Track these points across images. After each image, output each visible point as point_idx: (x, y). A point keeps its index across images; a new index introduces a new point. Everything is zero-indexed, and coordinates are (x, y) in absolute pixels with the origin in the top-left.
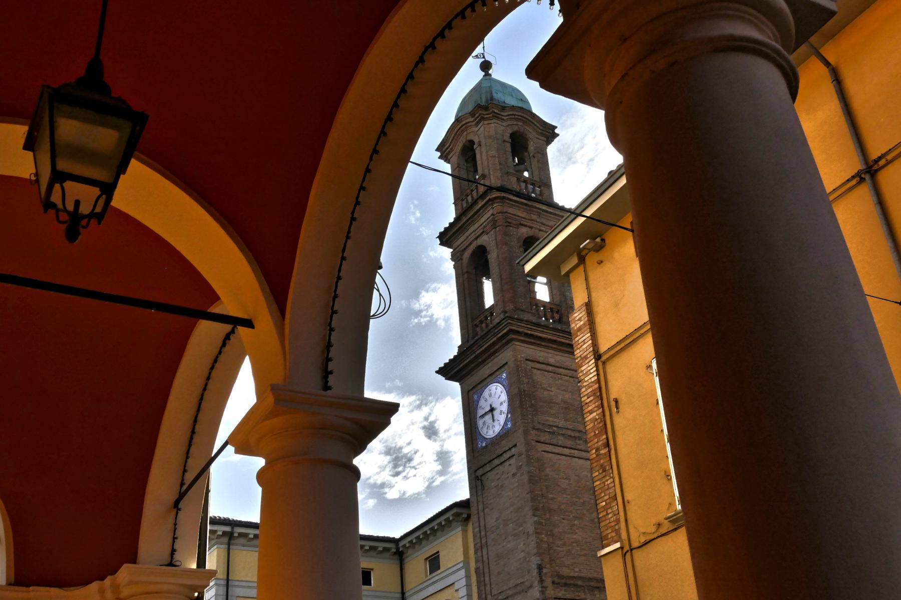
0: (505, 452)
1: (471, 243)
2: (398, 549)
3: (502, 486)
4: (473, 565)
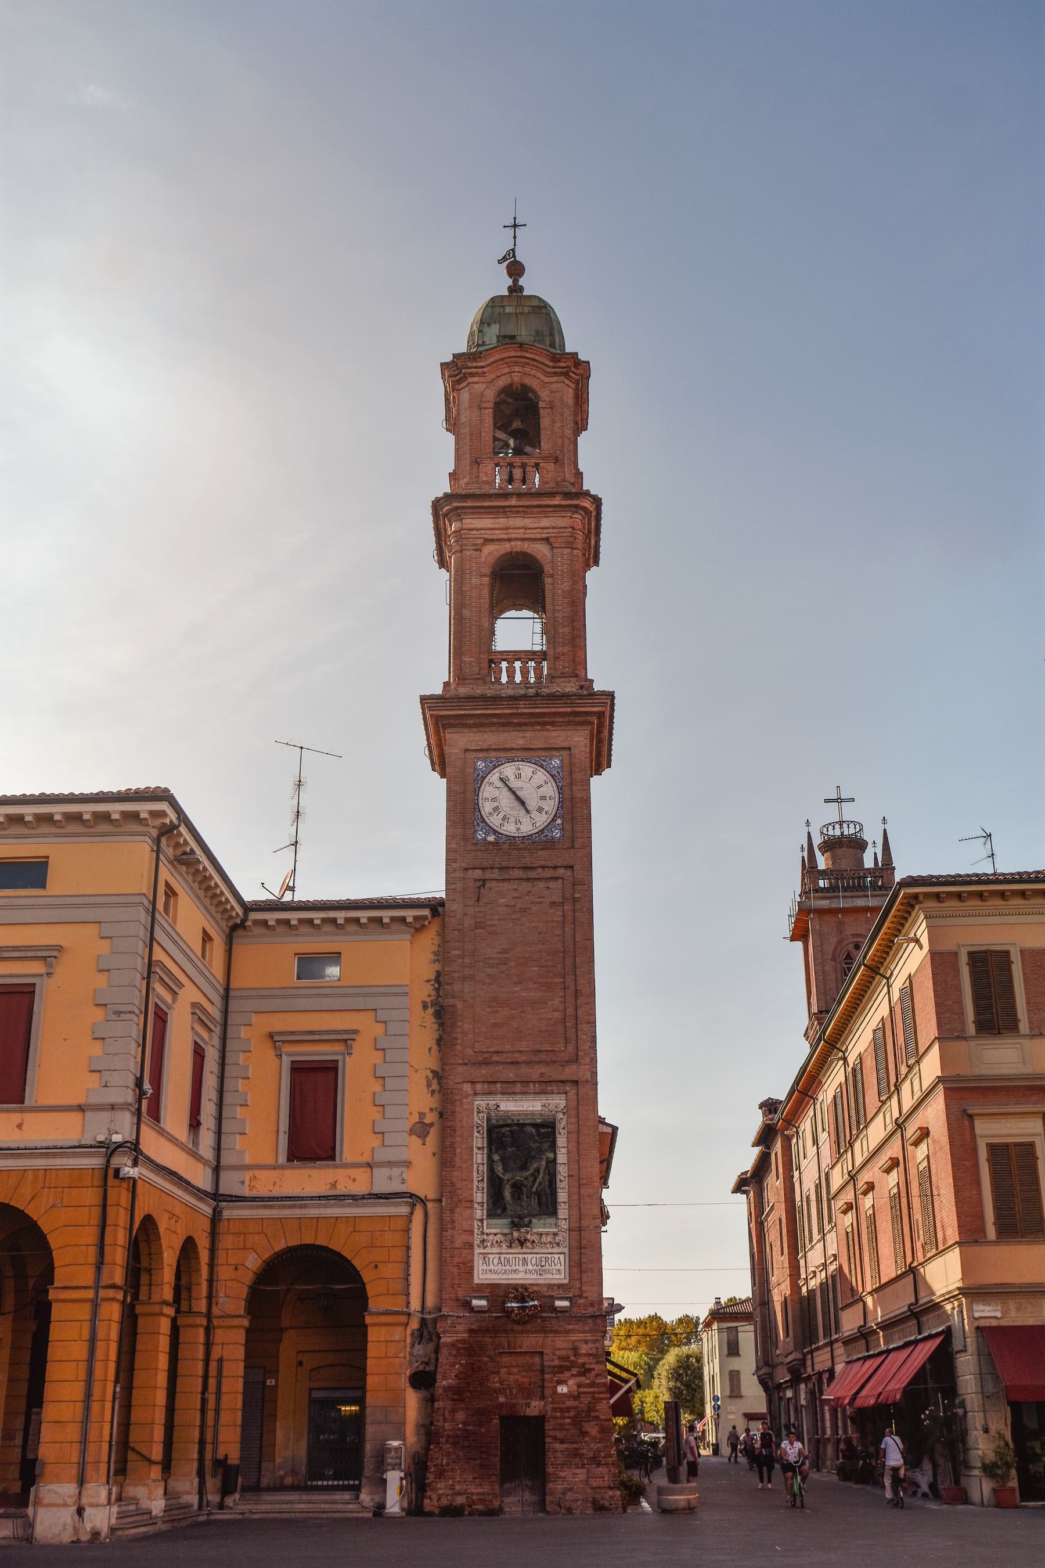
0: (543, 867)
1: (509, 540)
3: (523, 910)
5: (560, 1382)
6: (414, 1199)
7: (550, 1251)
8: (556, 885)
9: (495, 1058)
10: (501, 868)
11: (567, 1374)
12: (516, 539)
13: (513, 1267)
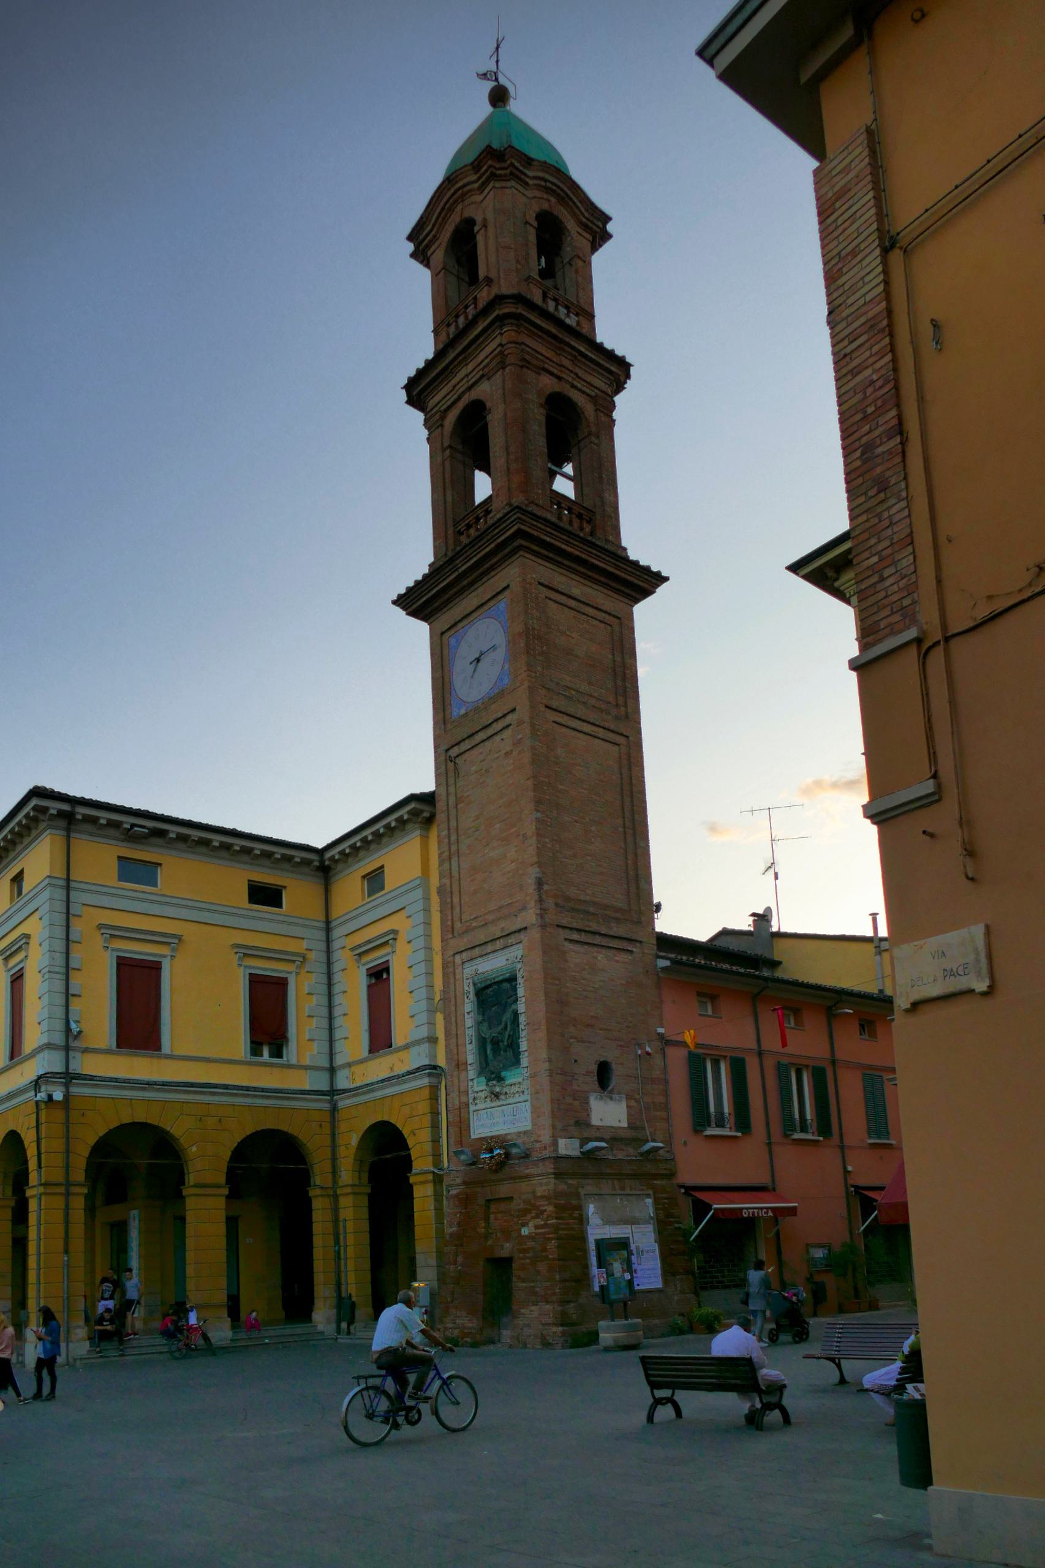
0: (496, 720)
1: (459, 398)
3: (487, 771)
4: (435, 881)
5: (524, 1225)
8: (507, 734)
10: (469, 737)
11: (528, 1217)
12: (463, 393)
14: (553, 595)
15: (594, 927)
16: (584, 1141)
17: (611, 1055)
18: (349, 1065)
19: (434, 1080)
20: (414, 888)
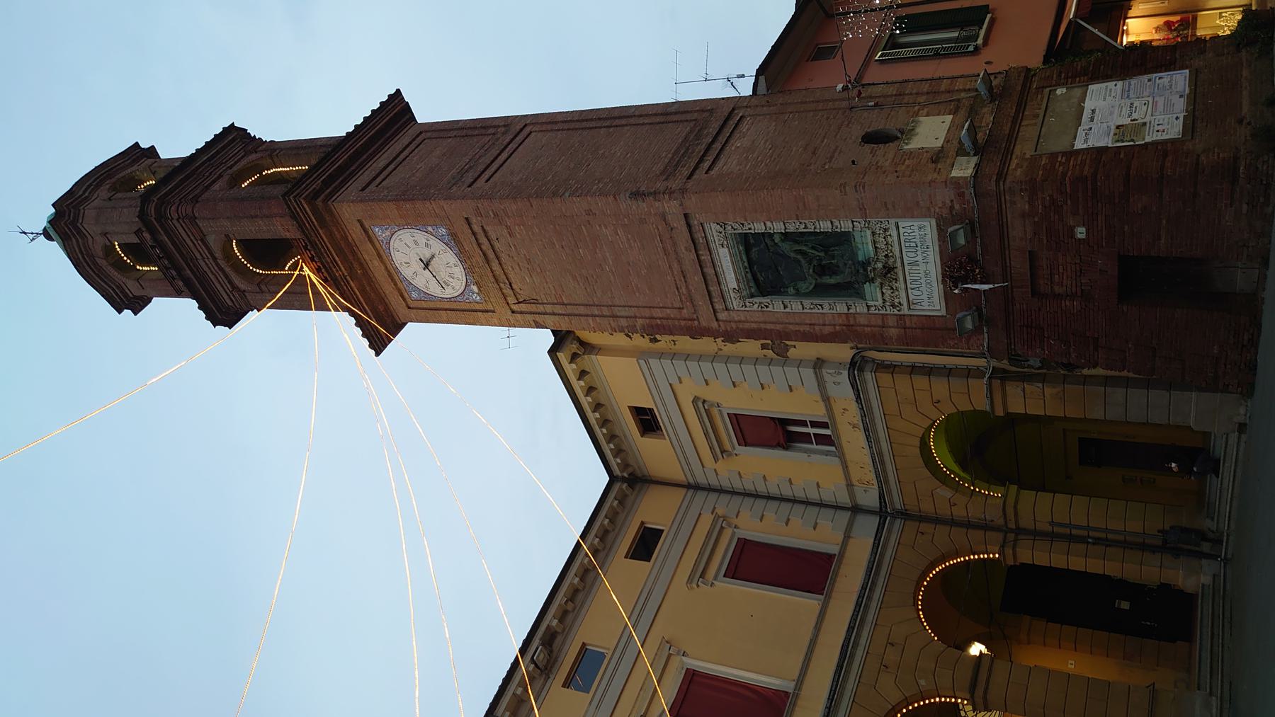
0: (479, 245)
1: (221, 269)
2: (623, 479)
3: (529, 262)
5: (1071, 233)
6: (856, 366)
7: (896, 238)
9: (684, 290)
12: (218, 265)
13: (922, 275)
14: (379, 180)
15: (703, 147)
16: (961, 152)
17: (857, 132)
18: (850, 485)
19: (869, 366)
20: (650, 369)
